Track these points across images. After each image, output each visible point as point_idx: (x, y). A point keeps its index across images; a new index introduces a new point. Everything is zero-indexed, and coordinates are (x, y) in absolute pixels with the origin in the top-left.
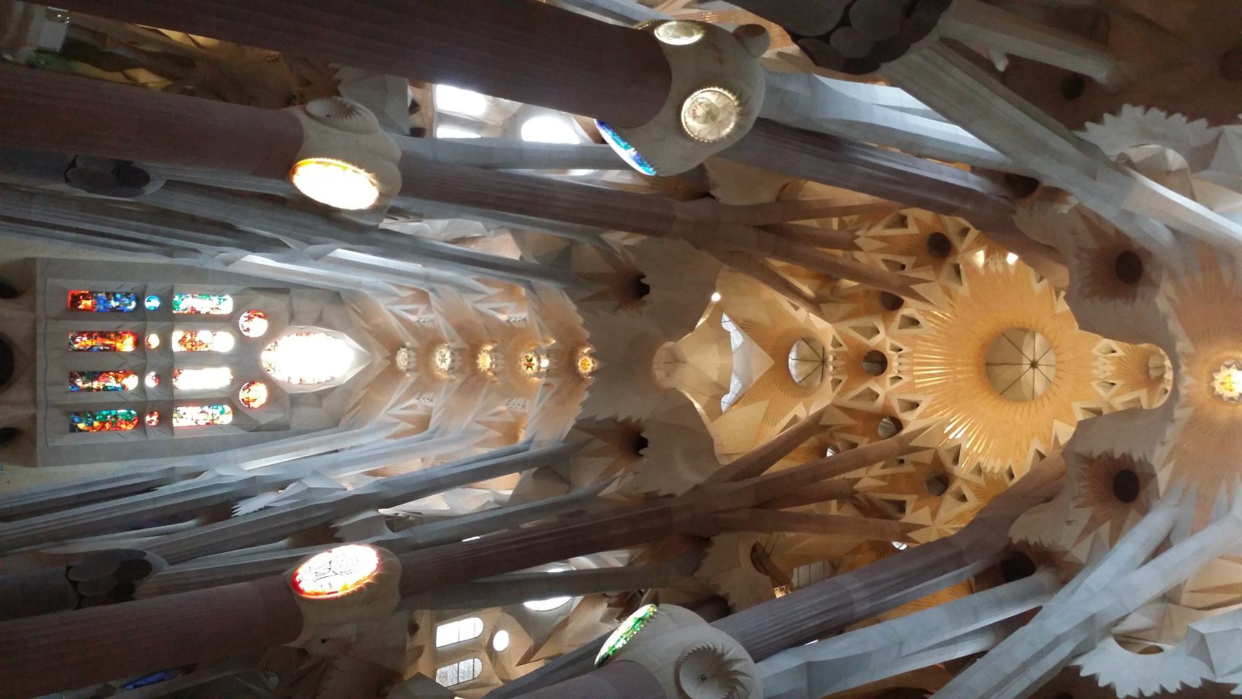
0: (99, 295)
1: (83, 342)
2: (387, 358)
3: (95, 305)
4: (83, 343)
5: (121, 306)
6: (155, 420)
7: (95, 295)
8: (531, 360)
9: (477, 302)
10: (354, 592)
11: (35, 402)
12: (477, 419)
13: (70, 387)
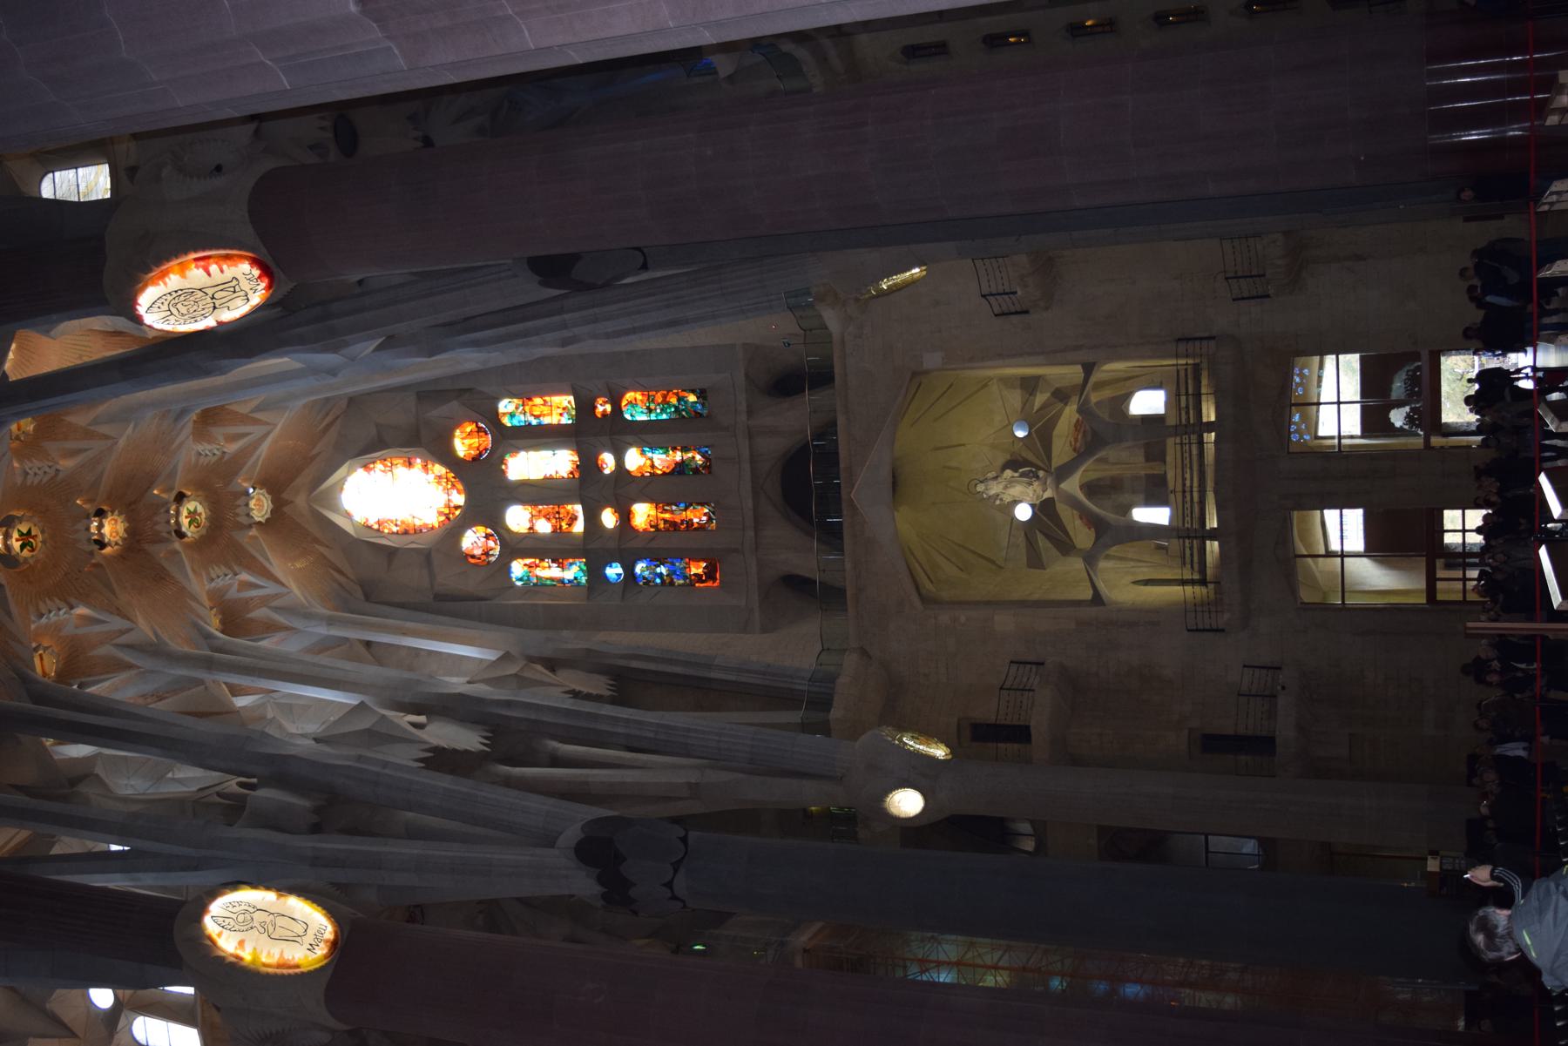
0: (681, 582)
1: (698, 516)
2: (287, 503)
3: (685, 568)
4: (698, 514)
5: (653, 567)
6: (599, 406)
7: (688, 581)
8: (22, 547)
9: (129, 630)
10: (168, 259)
11: (751, 435)
12: (109, 442)
13: (710, 452)
